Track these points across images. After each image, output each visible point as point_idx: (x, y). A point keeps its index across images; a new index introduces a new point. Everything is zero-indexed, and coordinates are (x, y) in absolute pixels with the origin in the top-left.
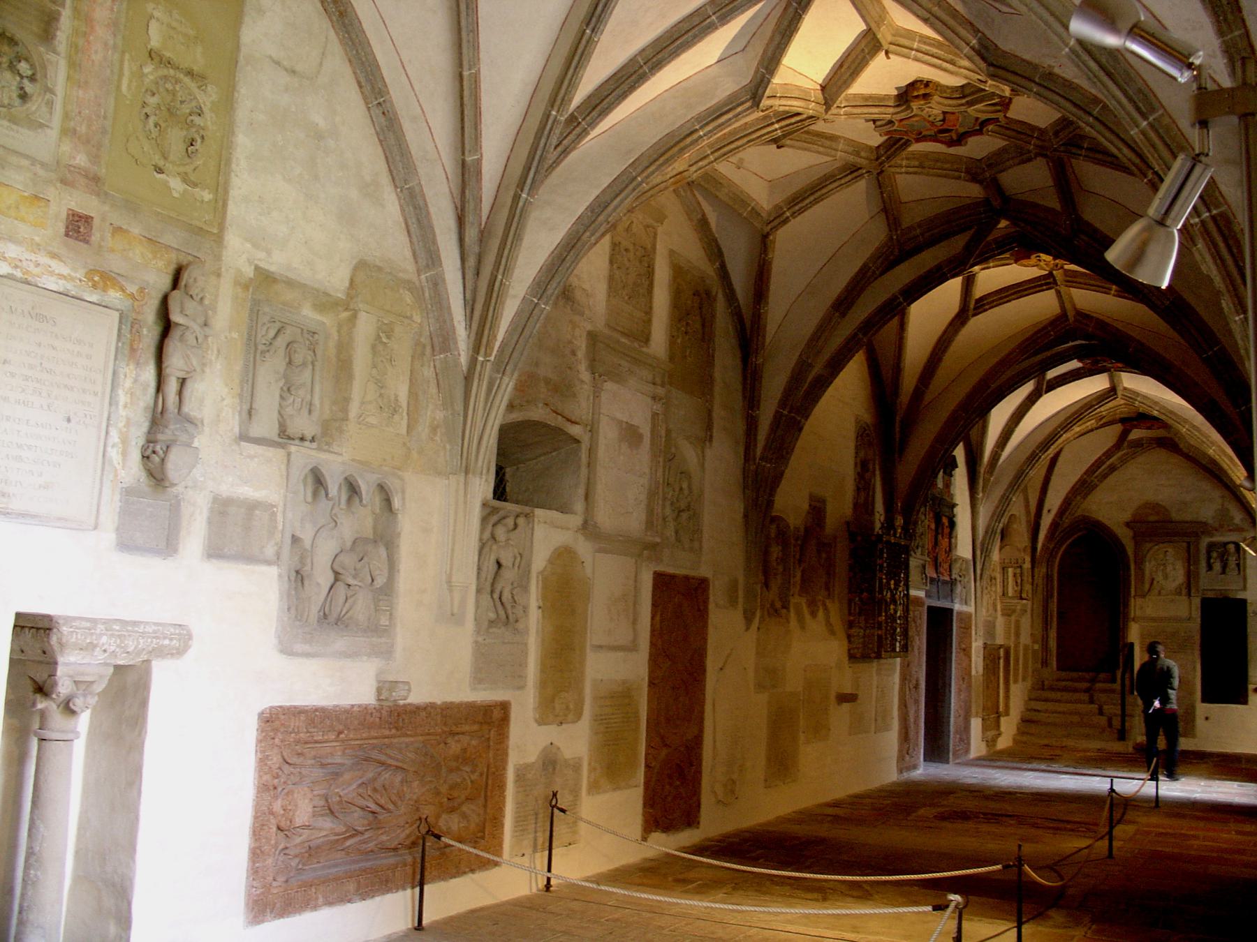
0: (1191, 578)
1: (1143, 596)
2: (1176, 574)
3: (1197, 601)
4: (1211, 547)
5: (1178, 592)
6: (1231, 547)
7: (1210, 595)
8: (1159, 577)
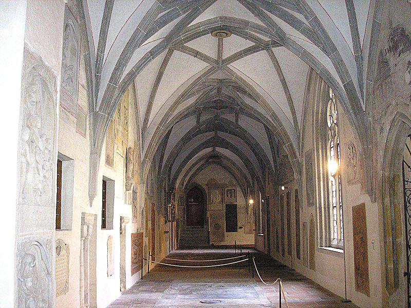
5: (219, 203)
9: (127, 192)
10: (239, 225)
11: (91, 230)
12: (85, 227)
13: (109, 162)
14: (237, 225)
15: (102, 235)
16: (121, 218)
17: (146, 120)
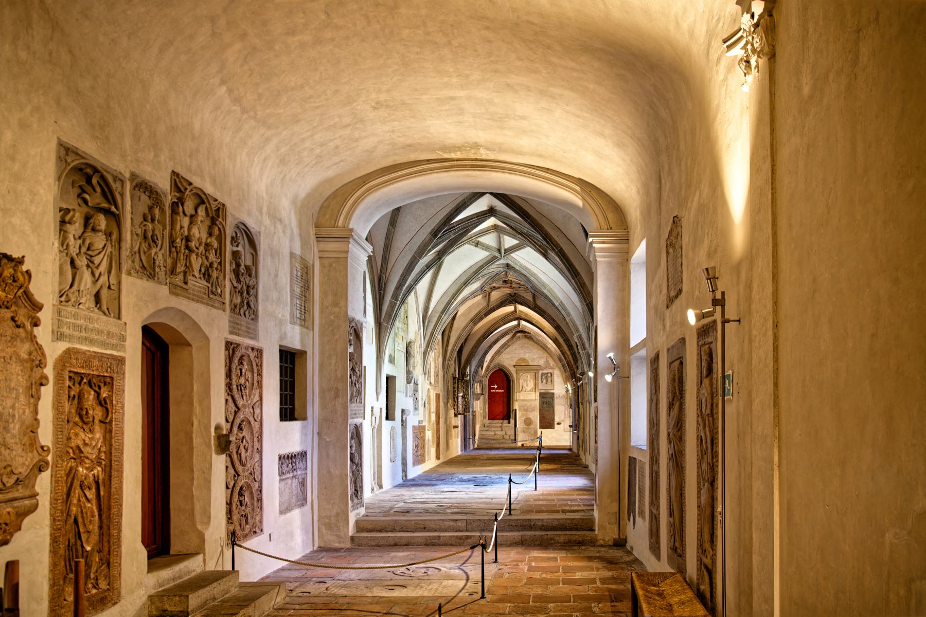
0: (536, 385)
1: (520, 392)
2: (531, 384)
3: (538, 394)
5: (531, 390)
7: (542, 391)
8: (525, 385)
13: (392, 360)
14: (553, 420)
15: (387, 425)
16: (403, 411)
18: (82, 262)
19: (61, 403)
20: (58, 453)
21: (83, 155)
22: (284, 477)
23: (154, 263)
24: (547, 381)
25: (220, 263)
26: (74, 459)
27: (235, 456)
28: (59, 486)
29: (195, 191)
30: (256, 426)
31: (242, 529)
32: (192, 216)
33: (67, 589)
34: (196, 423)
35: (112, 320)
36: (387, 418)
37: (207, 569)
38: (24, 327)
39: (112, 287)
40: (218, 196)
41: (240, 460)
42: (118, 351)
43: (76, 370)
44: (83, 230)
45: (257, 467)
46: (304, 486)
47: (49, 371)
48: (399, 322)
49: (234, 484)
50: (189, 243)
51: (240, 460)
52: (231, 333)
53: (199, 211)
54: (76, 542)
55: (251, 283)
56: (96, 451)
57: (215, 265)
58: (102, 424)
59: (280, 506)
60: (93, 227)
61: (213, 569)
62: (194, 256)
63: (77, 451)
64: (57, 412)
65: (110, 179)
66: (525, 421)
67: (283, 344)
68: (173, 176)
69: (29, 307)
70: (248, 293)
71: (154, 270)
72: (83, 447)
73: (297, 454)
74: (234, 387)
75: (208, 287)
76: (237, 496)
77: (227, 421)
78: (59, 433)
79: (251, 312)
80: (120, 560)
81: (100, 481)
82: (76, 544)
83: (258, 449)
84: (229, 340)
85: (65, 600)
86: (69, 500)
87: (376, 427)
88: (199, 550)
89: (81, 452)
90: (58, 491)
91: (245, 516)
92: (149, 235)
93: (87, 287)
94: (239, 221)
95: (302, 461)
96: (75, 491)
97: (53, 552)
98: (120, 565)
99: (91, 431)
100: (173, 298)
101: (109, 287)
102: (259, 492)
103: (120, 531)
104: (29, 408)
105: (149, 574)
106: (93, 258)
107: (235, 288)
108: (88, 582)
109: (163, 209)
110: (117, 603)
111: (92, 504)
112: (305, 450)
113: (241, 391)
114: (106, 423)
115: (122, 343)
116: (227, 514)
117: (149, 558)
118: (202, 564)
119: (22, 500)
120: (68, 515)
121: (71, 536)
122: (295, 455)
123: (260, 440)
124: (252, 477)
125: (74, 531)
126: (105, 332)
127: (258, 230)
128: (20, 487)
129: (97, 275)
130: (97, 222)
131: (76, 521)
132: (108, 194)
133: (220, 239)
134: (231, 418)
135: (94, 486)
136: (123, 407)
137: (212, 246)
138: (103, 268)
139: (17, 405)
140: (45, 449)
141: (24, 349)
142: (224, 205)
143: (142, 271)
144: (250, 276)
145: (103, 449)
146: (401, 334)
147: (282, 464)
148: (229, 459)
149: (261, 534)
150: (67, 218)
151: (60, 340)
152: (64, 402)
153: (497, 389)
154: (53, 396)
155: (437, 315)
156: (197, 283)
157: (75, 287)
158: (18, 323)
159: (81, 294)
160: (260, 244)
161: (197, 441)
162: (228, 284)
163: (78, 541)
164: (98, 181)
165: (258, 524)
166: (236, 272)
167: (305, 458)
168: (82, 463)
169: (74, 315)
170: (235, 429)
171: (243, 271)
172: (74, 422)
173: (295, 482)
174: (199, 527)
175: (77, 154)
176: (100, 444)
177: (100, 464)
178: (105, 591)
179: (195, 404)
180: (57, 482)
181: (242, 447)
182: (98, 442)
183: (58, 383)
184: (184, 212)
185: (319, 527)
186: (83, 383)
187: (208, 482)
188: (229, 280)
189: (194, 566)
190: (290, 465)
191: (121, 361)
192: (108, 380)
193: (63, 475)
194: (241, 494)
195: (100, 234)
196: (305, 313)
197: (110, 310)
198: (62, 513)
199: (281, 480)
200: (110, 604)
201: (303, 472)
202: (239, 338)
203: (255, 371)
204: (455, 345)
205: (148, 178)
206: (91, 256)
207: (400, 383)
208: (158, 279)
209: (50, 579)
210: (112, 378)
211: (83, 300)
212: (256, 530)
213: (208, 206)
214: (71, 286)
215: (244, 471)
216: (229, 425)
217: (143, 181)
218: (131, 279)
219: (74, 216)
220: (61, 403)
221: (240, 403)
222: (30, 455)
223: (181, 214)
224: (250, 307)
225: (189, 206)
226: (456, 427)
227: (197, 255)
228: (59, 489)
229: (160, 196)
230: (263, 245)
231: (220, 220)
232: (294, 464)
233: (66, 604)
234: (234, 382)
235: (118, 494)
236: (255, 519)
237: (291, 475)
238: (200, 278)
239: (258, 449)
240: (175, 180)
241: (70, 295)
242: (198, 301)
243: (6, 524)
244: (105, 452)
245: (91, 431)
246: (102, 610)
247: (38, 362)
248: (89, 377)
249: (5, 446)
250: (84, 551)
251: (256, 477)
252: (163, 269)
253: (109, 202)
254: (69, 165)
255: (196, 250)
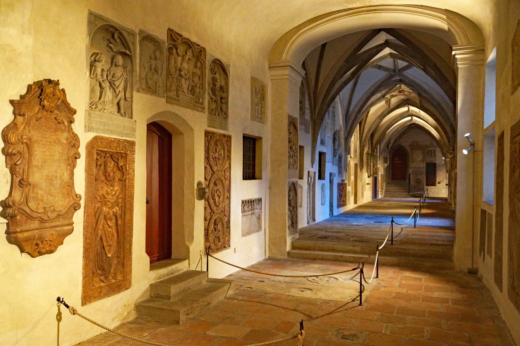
0: (424, 158)
2: (420, 158)
4: (428, 151)
6: (433, 151)
7: (428, 162)
9: (335, 158)
10: (438, 180)
11: (312, 180)
12: (310, 178)
13: (323, 143)
15: (318, 183)
16: (330, 174)
17: (348, 111)
18: (106, 85)
19: (91, 169)
20: (89, 199)
21: (107, 20)
22: (245, 214)
23: (156, 84)
24: (431, 155)
25: (202, 84)
26: (101, 202)
27: (211, 201)
28: (89, 218)
29: (184, 40)
30: (227, 182)
31: (216, 245)
32: (183, 56)
33: (95, 280)
34: (186, 181)
35: (126, 119)
36: (320, 178)
37: (191, 269)
38: (63, 123)
39: (128, 99)
40: (200, 43)
41: (215, 203)
42: (130, 137)
43: (101, 149)
44: (110, 66)
45: (227, 208)
46: (260, 219)
47: (82, 150)
48: (329, 119)
49: (210, 218)
50: (181, 72)
51: (215, 203)
52: (209, 126)
53: (188, 53)
54: (101, 251)
55: (224, 96)
56: (115, 197)
57: (198, 85)
58: (120, 181)
59: (242, 231)
60: (115, 64)
61: (194, 269)
62: (183, 80)
63: (103, 198)
64: (88, 174)
65: (125, 34)
66: (416, 180)
67: (246, 133)
68: (169, 32)
69: (67, 111)
70: (221, 102)
71: (156, 89)
72: (107, 195)
73: (254, 200)
74: (211, 159)
75: (193, 99)
76: (213, 225)
77: (206, 179)
78: (90, 187)
79: (223, 113)
80: (131, 263)
81: (118, 216)
82: (101, 253)
83: (227, 196)
84: (207, 131)
85: (93, 286)
86: (97, 226)
87: (312, 183)
88: (186, 257)
89: (105, 198)
90: (89, 221)
91: (218, 237)
92: (153, 68)
93: (109, 100)
94: (215, 58)
95: (259, 204)
96: (100, 222)
97: (85, 257)
98: (131, 265)
99: (112, 186)
100: (169, 105)
101: (125, 99)
102: (228, 223)
103: (131, 245)
104: (67, 171)
105: (151, 271)
106: (115, 82)
107: (212, 99)
108: (110, 276)
109: (162, 52)
110: (129, 288)
111: (113, 229)
112: (260, 197)
113: (216, 162)
114: (123, 181)
115: (134, 133)
116: (205, 235)
117: (151, 262)
118: (188, 266)
119: (62, 227)
120: (97, 236)
121: (99, 247)
122: (253, 201)
123: (229, 191)
124: (223, 214)
125: (100, 245)
126: (122, 126)
127: (228, 63)
128: (61, 219)
129: (117, 93)
130: (117, 60)
131: (101, 239)
132: (125, 43)
133: (202, 68)
134: (208, 178)
135: (114, 218)
136: (134, 171)
137: (197, 74)
138: (121, 88)
139: (59, 170)
140: (78, 196)
141: (64, 137)
142: (204, 48)
143: (148, 89)
144: (223, 92)
145: (121, 196)
146: (330, 126)
147: (244, 206)
148: (207, 202)
149: (229, 248)
150: (97, 59)
151: (90, 131)
152: (93, 168)
153: (398, 160)
154: (86, 165)
155: (354, 114)
156: (186, 96)
157: (102, 100)
158: (59, 121)
159: (105, 104)
160: (229, 72)
161: (186, 191)
162: (207, 96)
163: (103, 250)
164: (118, 36)
165: (227, 242)
166: (213, 90)
167: (260, 203)
168: (106, 204)
169: (100, 116)
170: (212, 185)
171: (218, 89)
172: (101, 180)
173: (254, 217)
174: (187, 244)
175: (103, 20)
176: (118, 193)
177: (118, 205)
178: (120, 281)
179: (185, 169)
180: (88, 216)
181: (216, 195)
182: (116, 192)
183: (89, 157)
184: (177, 53)
185: (269, 245)
186: (106, 157)
187: (192, 216)
188: (208, 94)
189: (182, 267)
190: (250, 207)
191: (133, 144)
192: (124, 155)
193: (92, 212)
194: (215, 224)
195: (120, 68)
196: (261, 114)
197: (126, 113)
198: (91, 234)
199: (243, 216)
200: (124, 289)
201: (259, 211)
202: (215, 129)
203: (226, 149)
204: (368, 133)
205: (151, 33)
206: (114, 81)
207: (329, 157)
208: (159, 94)
209: (83, 274)
210: (126, 154)
211: (107, 108)
212: (226, 245)
213: (193, 49)
214: (100, 98)
215: (217, 210)
216: (207, 183)
217: (148, 35)
218: (139, 94)
219: (100, 57)
220: (91, 169)
221: (215, 169)
222: (68, 200)
223: (175, 54)
224: (223, 111)
225: (182, 49)
226: (368, 184)
227: (186, 79)
228: (89, 220)
229: (160, 44)
230: (232, 72)
231: (202, 57)
232: (253, 206)
233: (95, 288)
234: (211, 156)
235: (129, 223)
236: (225, 239)
237: (251, 213)
238: (188, 93)
239: (227, 196)
240: (171, 34)
241: (98, 104)
242: (187, 107)
243: (51, 241)
244: (122, 198)
245: (112, 186)
246: (119, 292)
247: (73, 144)
248: (111, 153)
249: (50, 194)
250: (107, 257)
251: (227, 213)
252: (162, 88)
253: (126, 48)
254: (97, 25)
255: (185, 76)
